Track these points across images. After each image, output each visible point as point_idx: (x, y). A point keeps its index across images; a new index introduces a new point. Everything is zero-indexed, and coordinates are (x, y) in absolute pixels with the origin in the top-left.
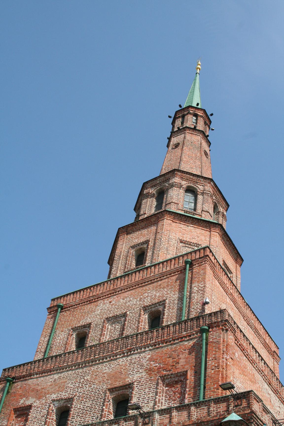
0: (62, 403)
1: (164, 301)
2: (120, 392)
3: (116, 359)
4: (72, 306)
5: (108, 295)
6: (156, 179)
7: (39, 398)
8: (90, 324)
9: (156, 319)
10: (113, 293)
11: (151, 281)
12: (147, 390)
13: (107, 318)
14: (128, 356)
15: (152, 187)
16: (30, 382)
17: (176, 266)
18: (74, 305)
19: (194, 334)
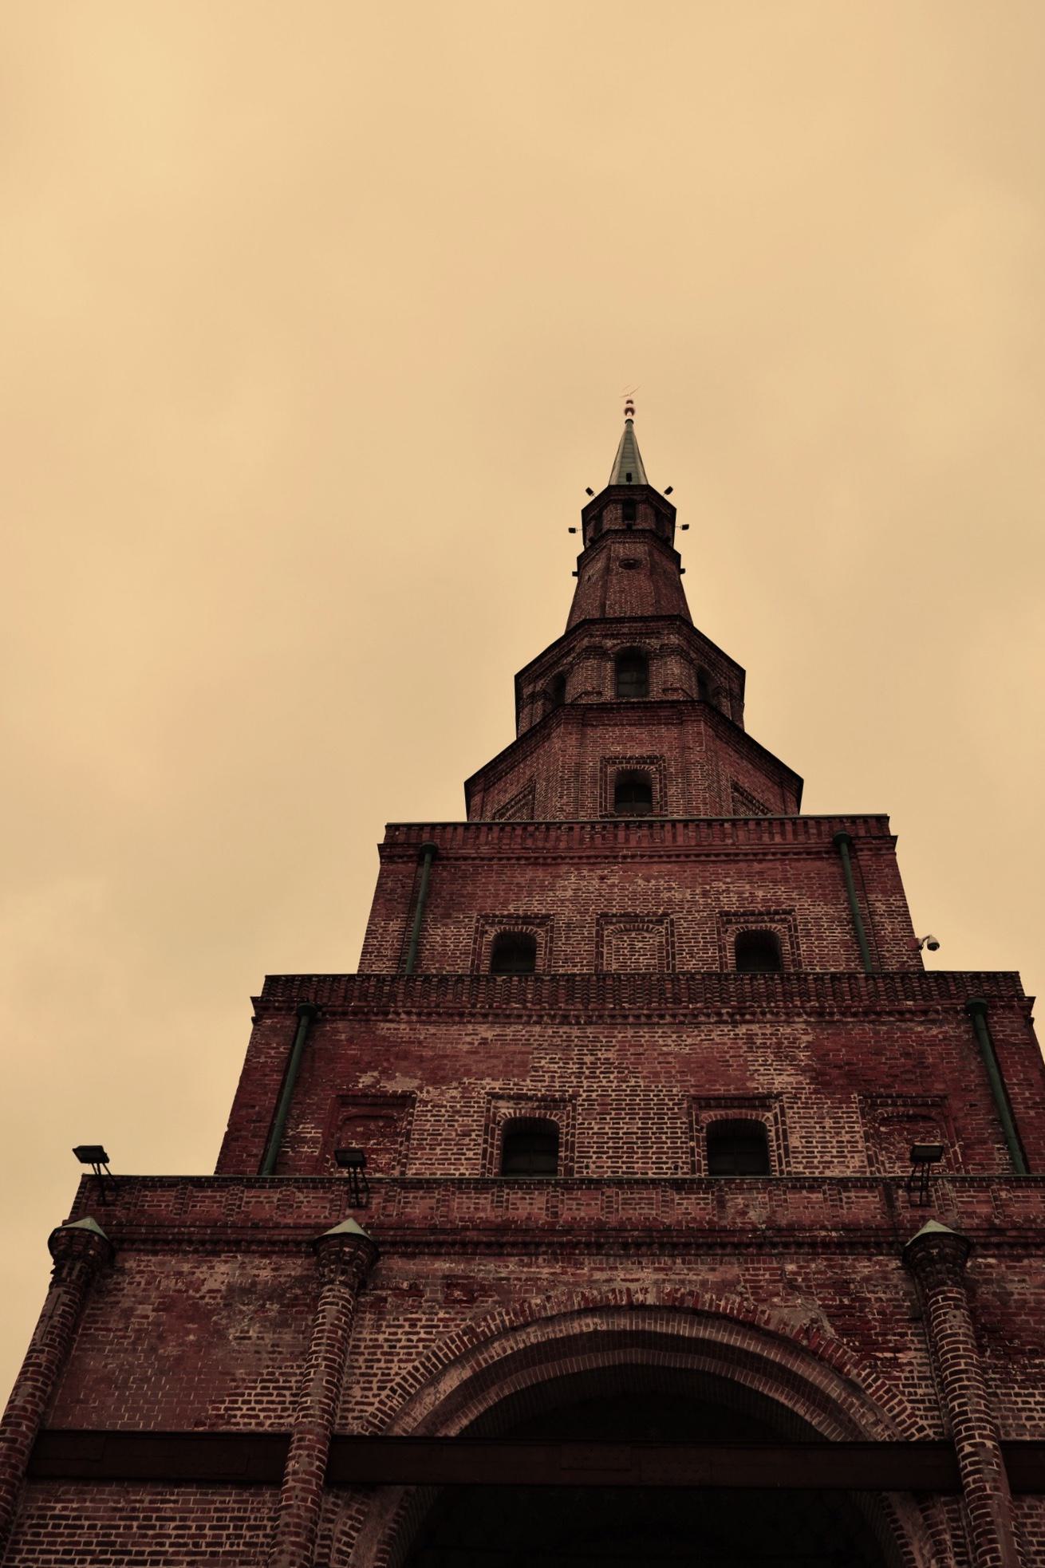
0: (525, 1110)
1: (789, 913)
2: (732, 1113)
3: (698, 1025)
4: (465, 859)
5: (588, 857)
6: (620, 620)
7: (436, 1078)
8: (547, 916)
9: (758, 950)
10: (606, 857)
11: (731, 858)
12: (828, 1123)
13: (604, 915)
14: (735, 1024)
15: (605, 636)
16: (384, 1028)
17: (802, 838)
18: (474, 859)
19: (937, 1012)
